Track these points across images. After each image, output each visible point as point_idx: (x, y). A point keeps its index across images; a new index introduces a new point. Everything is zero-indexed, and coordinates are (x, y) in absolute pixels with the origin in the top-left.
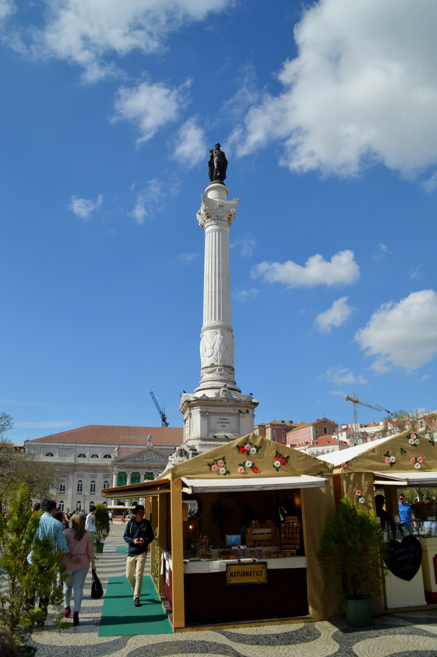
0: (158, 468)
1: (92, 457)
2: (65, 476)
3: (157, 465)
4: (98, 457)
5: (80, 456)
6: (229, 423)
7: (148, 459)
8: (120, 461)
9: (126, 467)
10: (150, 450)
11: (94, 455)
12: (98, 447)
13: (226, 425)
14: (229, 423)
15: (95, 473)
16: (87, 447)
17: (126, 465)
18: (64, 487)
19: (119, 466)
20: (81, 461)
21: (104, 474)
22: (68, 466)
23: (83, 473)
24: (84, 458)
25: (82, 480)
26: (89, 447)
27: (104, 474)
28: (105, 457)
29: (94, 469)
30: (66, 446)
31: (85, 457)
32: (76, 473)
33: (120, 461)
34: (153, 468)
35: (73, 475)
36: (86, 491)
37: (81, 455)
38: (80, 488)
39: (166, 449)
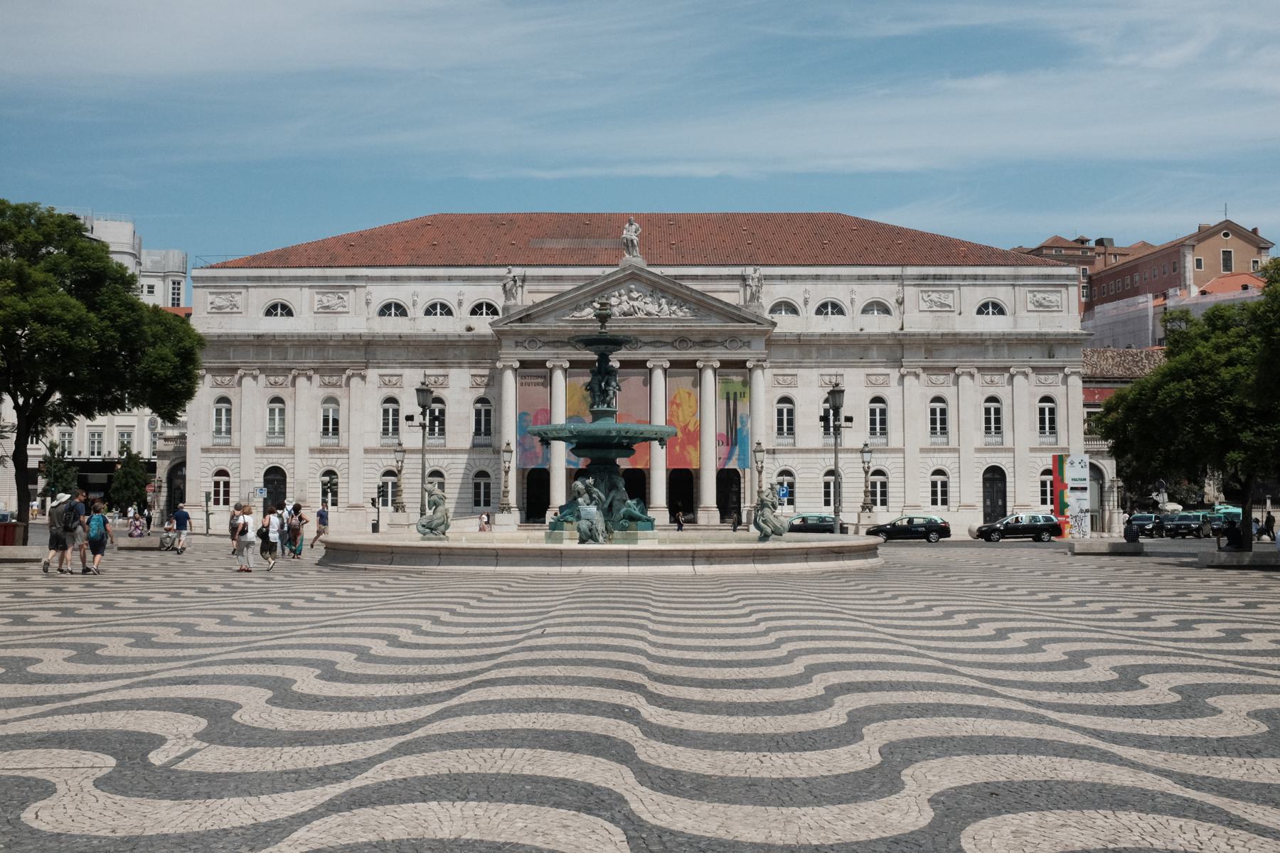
0: (665, 344)
1: (428, 313)
2: (334, 385)
3: (662, 333)
4: (449, 313)
5: (385, 310)
7: (625, 307)
8: (520, 320)
9: (546, 344)
10: (634, 276)
11: (434, 306)
12: (450, 279)
15: (441, 371)
17: (543, 333)
18: (336, 422)
19: (520, 339)
20: (393, 326)
22: (345, 347)
23: (398, 371)
24: (400, 319)
25: (397, 397)
27: (474, 371)
29: (437, 351)
30: (335, 278)
32: (372, 374)
34: (646, 344)
35: (363, 378)
36: (411, 437)
38: (391, 423)
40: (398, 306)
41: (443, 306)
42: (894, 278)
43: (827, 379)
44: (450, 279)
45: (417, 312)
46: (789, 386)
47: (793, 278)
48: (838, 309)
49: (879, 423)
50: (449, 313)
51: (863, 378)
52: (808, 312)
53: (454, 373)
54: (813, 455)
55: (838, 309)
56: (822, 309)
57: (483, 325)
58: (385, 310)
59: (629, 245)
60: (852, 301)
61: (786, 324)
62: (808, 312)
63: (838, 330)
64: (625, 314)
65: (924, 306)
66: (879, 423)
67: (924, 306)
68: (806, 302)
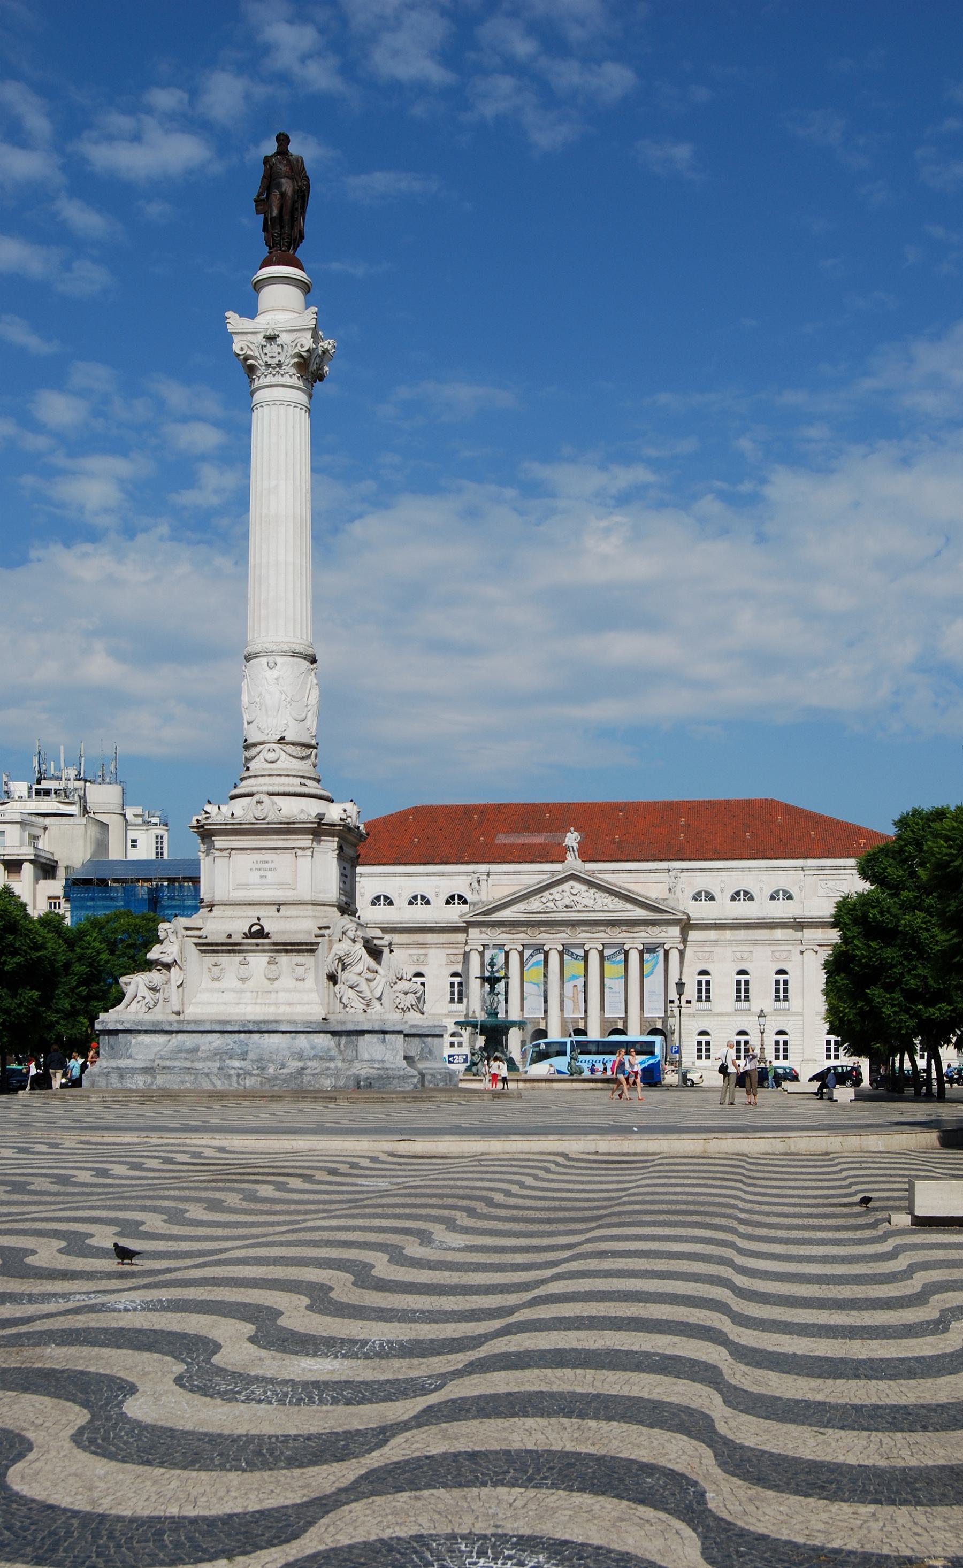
4: (428, 903)
6: (274, 869)
8: (483, 913)
10: (573, 877)
13: (269, 874)
14: (274, 869)
15: (422, 951)
16: (395, 874)
21: (450, 951)
26: (401, 875)
27: (450, 951)
28: (448, 902)
31: (391, 903)
33: (483, 913)
37: (378, 898)
39: (630, 871)
40: (386, 898)
41: (423, 897)
42: (795, 868)
43: (739, 955)
44: (428, 874)
45: (401, 901)
46: (707, 961)
47: (711, 870)
48: (749, 896)
49: (782, 992)
50: (428, 903)
51: (770, 953)
52: (723, 899)
53: (432, 952)
54: (726, 1019)
55: (749, 896)
56: (735, 897)
57: (455, 914)
58: (376, 901)
59: (567, 849)
60: (761, 889)
61: (699, 911)
62: (723, 899)
63: (749, 915)
64: (567, 907)
65: (822, 892)
66: (782, 992)
67: (822, 892)
68: (722, 891)
